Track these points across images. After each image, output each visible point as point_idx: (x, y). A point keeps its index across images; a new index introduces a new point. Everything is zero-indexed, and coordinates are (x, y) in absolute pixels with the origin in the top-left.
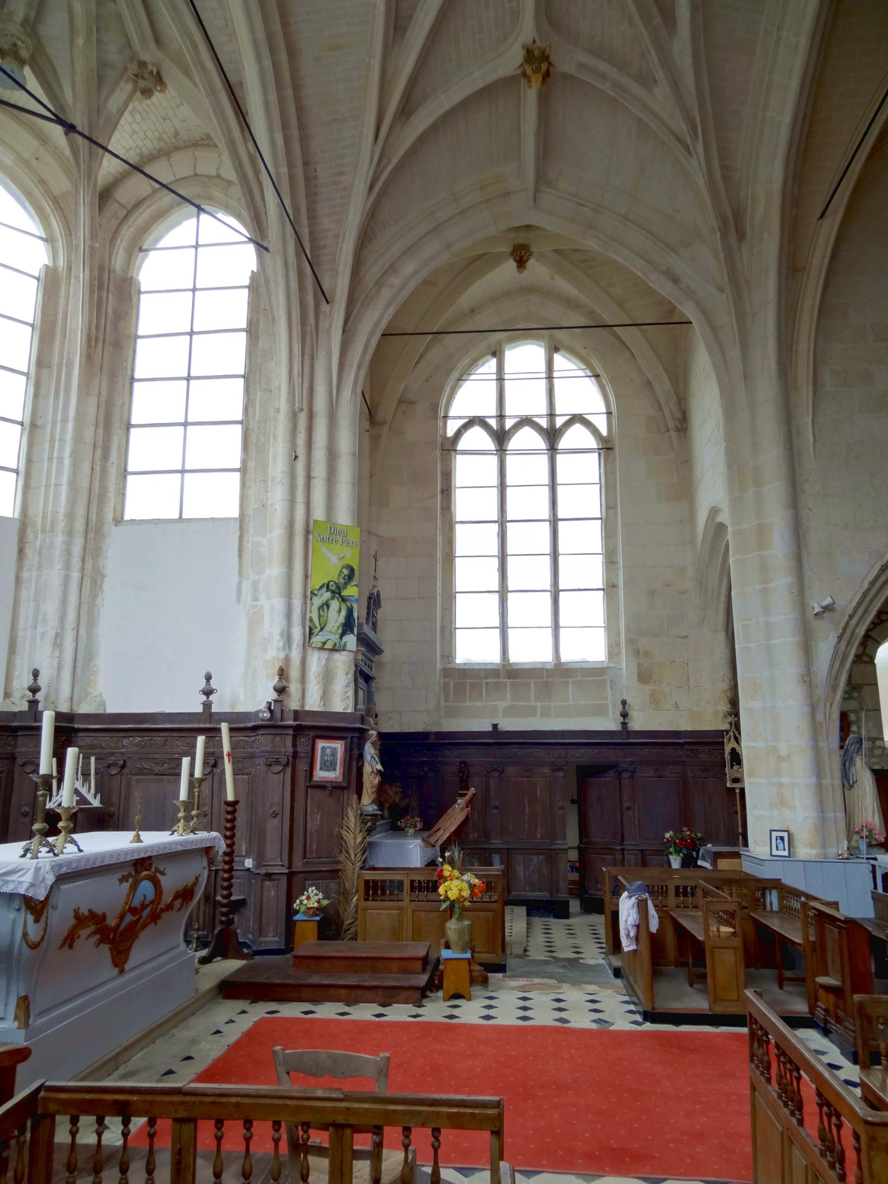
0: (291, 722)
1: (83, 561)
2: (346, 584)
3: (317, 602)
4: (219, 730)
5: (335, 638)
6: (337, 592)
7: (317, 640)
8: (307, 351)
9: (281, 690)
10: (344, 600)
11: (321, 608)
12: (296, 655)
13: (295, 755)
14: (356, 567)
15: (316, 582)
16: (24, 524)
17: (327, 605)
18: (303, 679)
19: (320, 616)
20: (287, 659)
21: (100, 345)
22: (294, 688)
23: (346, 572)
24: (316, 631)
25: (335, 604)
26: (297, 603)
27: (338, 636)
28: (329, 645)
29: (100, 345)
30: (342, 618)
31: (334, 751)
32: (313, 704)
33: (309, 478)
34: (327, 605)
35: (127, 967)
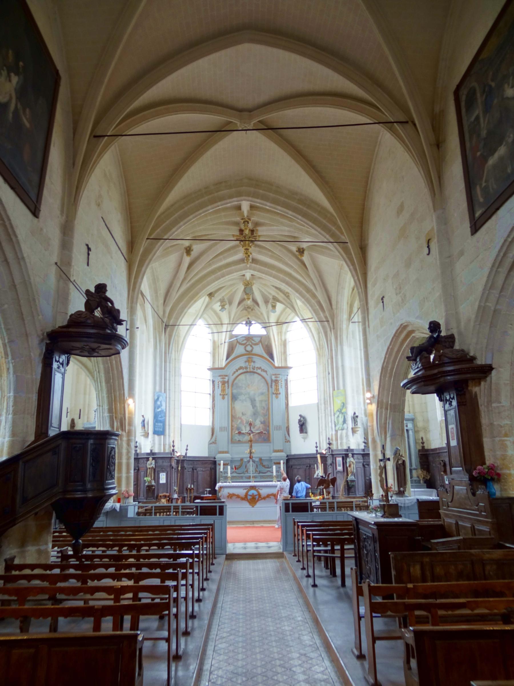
0: (331, 453)
1: (325, 410)
2: (343, 409)
3: (336, 416)
4: (317, 457)
5: (341, 426)
6: (340, 411)
7: (337, 428)
8: (329, 339)
9: (330, 444)
10: (342, 413)
11: (337, 418)
12: (334, 433)
13: (333, 462)
14: (344, 402)
15: (335, 411)
16: (318, 403)
17: (338, 416)
18: (337, 440)
19: (337, 420)
20: (332, 435)
21: (321, 350)
22: (334, 442)
23: (342, 404)
24: (337, 425)
25: (340, 415)
26: (333, 417)
27: (342, 425)
28: (340, 429)
29: (321, 350)
30: (342, 419)
31: (340, 461)
32: (340, 448)
33: (333, 378)
34: (338, 416)
35: (255, 506)
